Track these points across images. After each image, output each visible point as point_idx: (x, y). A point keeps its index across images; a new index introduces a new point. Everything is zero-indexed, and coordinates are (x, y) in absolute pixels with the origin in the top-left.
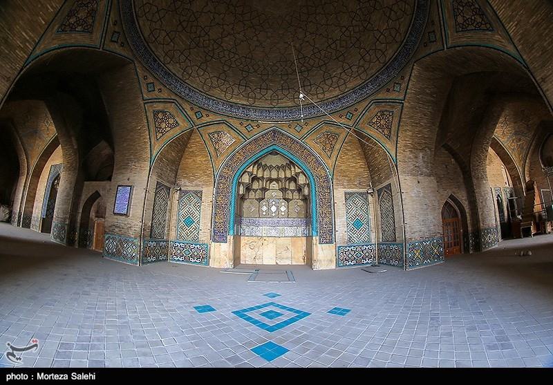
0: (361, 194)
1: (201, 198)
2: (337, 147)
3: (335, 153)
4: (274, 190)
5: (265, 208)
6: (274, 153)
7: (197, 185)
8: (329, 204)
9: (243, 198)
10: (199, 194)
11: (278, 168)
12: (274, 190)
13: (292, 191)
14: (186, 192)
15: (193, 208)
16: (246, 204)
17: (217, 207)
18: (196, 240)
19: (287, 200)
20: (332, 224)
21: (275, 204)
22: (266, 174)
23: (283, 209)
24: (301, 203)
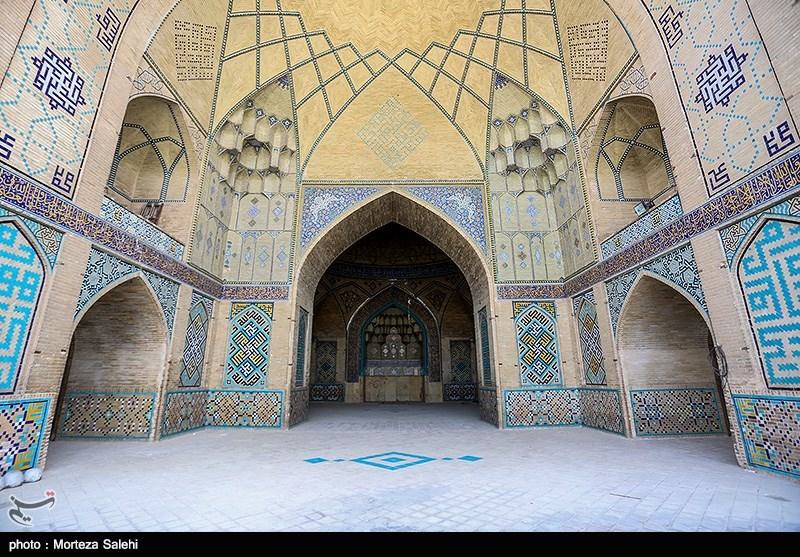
0: (464, 342)
1: (336, 347)
2: (444, 304)
3: (442, 309)
4: (394, 336)
5: (386, 351)
6: (394, 306)
7: (332, 337)
8: (438, 350)
9: (367, 343)
10: (334, 344)
11: (397, 317)
12: (394, 336)
13: (410, 335)
14: (323, 342)
15: (329, 356)
16: (369, 346)
17: (349, 353)
18: (333, 382)
19: (405, 343)
20: (439, 365)
21: (394, 347)
22: (387, 321)
23: (402, 351)
24: (418, 346)
